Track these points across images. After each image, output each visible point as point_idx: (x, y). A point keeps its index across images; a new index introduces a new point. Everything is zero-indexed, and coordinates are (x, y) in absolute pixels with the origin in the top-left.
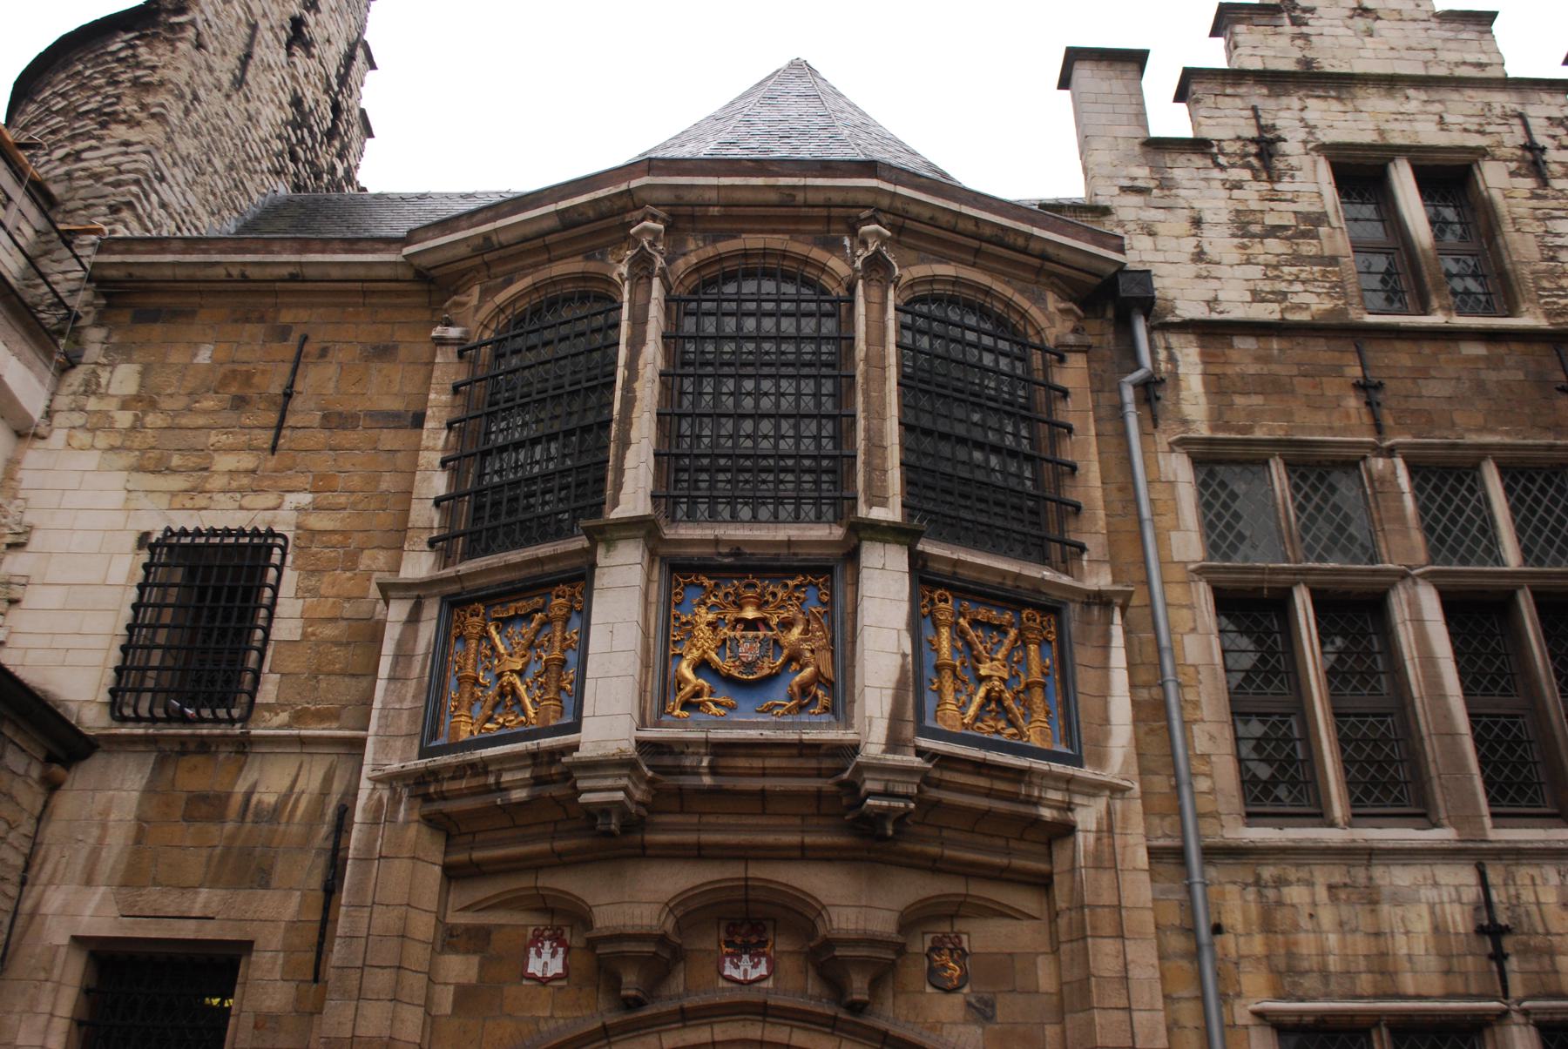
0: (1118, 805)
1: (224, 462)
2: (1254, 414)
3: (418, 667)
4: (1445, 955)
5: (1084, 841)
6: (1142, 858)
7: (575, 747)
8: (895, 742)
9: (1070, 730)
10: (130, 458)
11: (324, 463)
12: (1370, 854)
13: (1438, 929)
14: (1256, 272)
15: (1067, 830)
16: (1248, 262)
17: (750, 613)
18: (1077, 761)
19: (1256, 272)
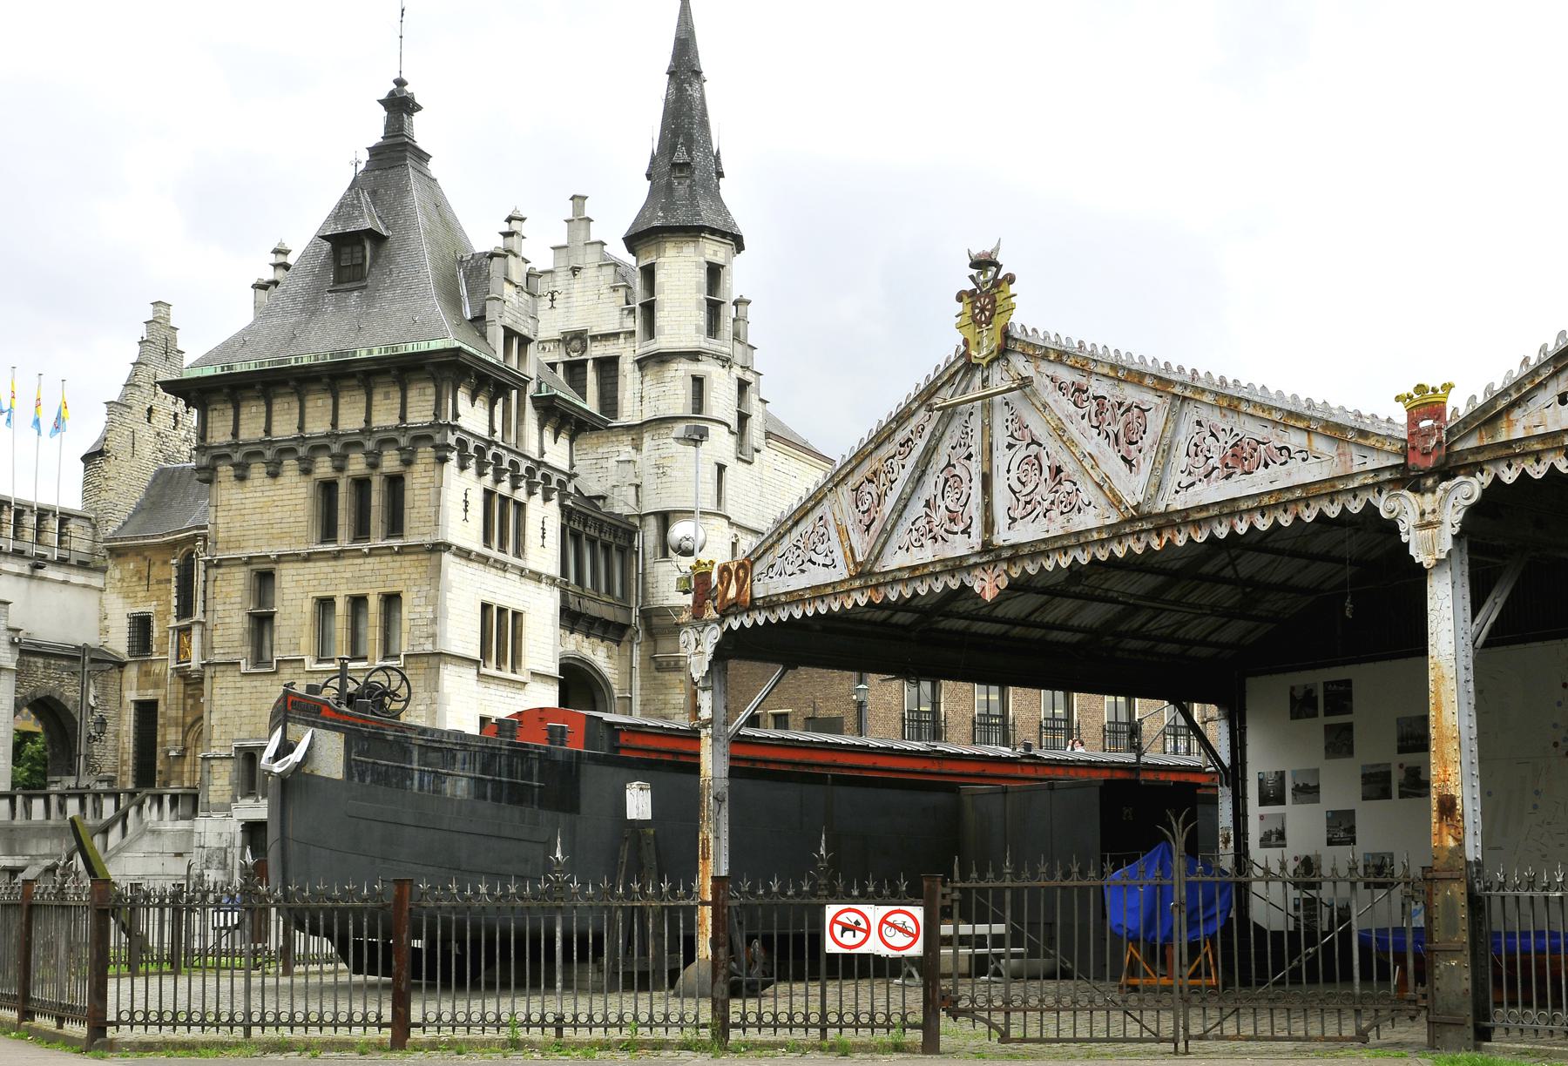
1: (140, 595)
3: (175, 645)
10: (122, 595)
11: (158, 593)
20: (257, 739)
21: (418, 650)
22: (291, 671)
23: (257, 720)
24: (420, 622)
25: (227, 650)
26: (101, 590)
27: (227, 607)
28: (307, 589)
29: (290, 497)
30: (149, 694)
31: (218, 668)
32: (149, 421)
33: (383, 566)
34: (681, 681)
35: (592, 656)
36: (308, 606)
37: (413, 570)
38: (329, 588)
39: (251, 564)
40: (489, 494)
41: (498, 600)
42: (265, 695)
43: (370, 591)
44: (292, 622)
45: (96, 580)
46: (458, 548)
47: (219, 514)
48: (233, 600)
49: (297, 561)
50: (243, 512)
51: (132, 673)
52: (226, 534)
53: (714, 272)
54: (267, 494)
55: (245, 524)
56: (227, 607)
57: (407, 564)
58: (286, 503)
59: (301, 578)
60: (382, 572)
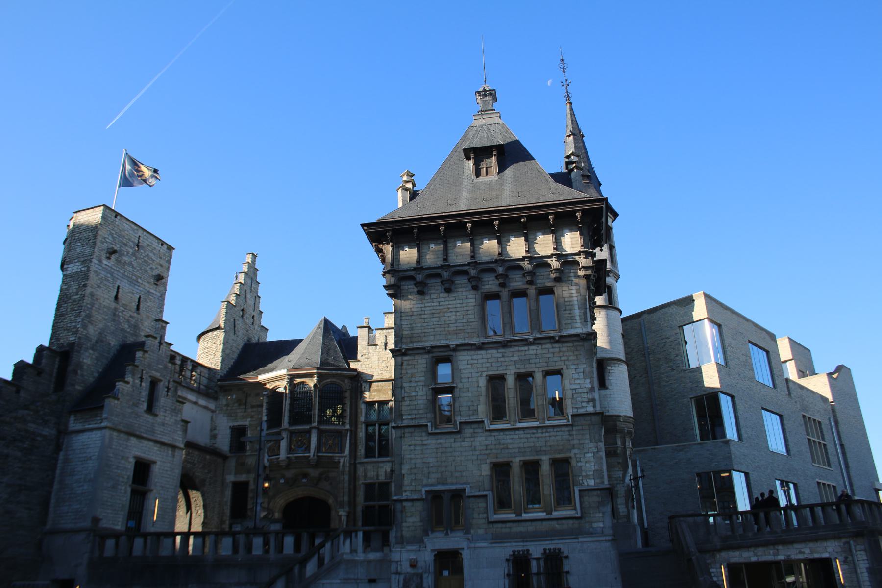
0: (346, 459)
2: (374, 396)
4: (386, 474)
5: (341, 464)
6: (348, 465)
7: (279, 458)
8: (314, 455)
9: (341, 450)
12: (378, 462)
13: (386, 472)
14: (379, 370)
15: (339, 462)
16: (379, 368)
17: (300, 438)
18: (341, 453)
19: (379, 370)
20: (444, 484)
21: (581, 411)
22: (471, 431)
23: (444, 469)
24: (580, 391)
25: (413, 416)
26: (213, 411)
27: (413, 384)
28: (481, 370)
29: (462, 305)
30: (243, 478)
31: (407, 430)
32: (234, 320)
33: (544, 351)
34: (619, 463)
36: (483, 382)
37: (571, 353)
38: (500, 368)
39: (432, 352)
42: (449, 450)
44: (470, 395)
45: (212, 406)
47: (403, 318)
48: (417, 379)
49: (471, 350)
50: (423, 316)
51: (232, 463)
52: (409, 332)
54: (441, 303)
55: (425, 324)
56: (413, 384)
57: (564, 349)
58: (458, 309)
59: (476, 361)
60: (544, 356)
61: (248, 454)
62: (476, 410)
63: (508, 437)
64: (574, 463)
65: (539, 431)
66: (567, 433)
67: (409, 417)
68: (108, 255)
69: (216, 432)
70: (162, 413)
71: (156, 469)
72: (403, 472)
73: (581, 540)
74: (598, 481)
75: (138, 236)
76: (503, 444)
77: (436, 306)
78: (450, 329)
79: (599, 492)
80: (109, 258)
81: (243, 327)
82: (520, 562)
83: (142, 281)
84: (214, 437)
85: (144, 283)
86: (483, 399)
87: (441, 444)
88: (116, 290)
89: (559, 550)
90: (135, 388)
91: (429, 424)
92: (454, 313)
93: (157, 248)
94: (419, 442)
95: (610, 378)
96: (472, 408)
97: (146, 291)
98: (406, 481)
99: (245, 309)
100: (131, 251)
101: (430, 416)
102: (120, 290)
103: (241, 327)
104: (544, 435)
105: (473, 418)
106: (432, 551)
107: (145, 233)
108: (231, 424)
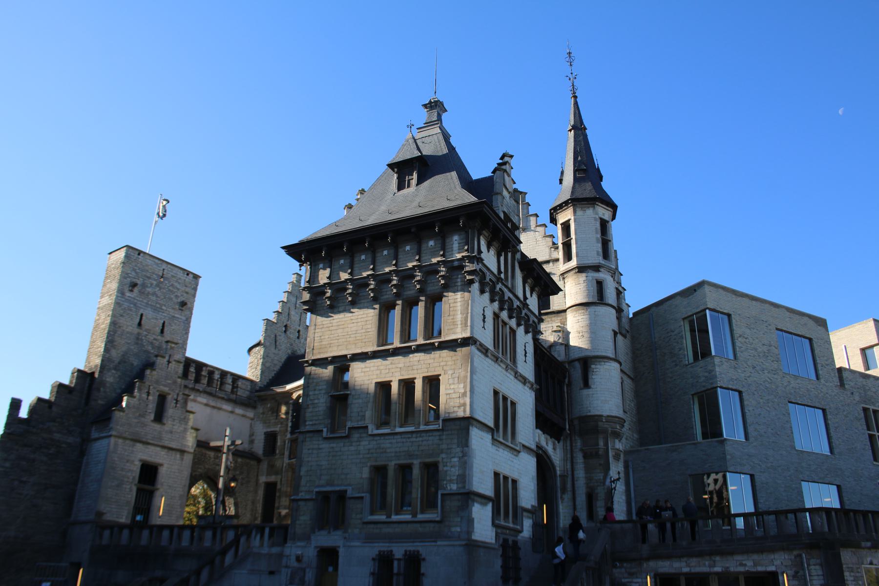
24: (454, 396)
25: (314, 422)
27: (317, 392)
29: (363, 316)
30: (272, 479)
31: (308, 435)
34: (600, 465)
35: (546, 447)
37: (449, 359)
38: (387, 375)
40: (496, 316)
41: (504, 390)
43: (417, 376)
46: (481, 345)
47: (317, 331)
48: (320, 388)
50: (331, 328)
51: (264, 466)
52: (319, 344)
53: (604, 226)
55: (332, 336)
56: (317, 392)
58: (359, 320)
59: (368, 369)
61: (277, 457)
62: (364, 416)
63: (387, 441)
64: (441, 467)
65: (414, 435)
66: (438, 438)
67: (311, 423)
68: (130, 288)
69: (254, 437)
70: (170, 422)
71: (163, 471)
72: (302, 473)
73: (439, 543)
74: (460, 485)
75: (162, 269)
76: (383, 449)
77: (342, 318)
78: (350, 339)
79: (460, 497)
80: (131, 291)
81: (286, 342)
82: (384, 560)
83: (167, 308)
84: (252, 442)
85: (168, 309)
86: (370, 405)
87: (333, 448)
88: (139, 318)
89: (418, 552)
90: (141, 401)
91: (325, 430)
92: (355, 324)
93: (182, 278)
94: (316, 446)
95: (593, 377)
96: (361, 414)
97: (170, 316)
98: (303, 482)
99: (288, 325)
100: (155, 283)
101: (328, 421)
102: (144, 318)
103: (283, 342)
104: (418, 439)
105: (361, 424)
106: (316, 547)
107: (169, 266)
108: (265, 430)
